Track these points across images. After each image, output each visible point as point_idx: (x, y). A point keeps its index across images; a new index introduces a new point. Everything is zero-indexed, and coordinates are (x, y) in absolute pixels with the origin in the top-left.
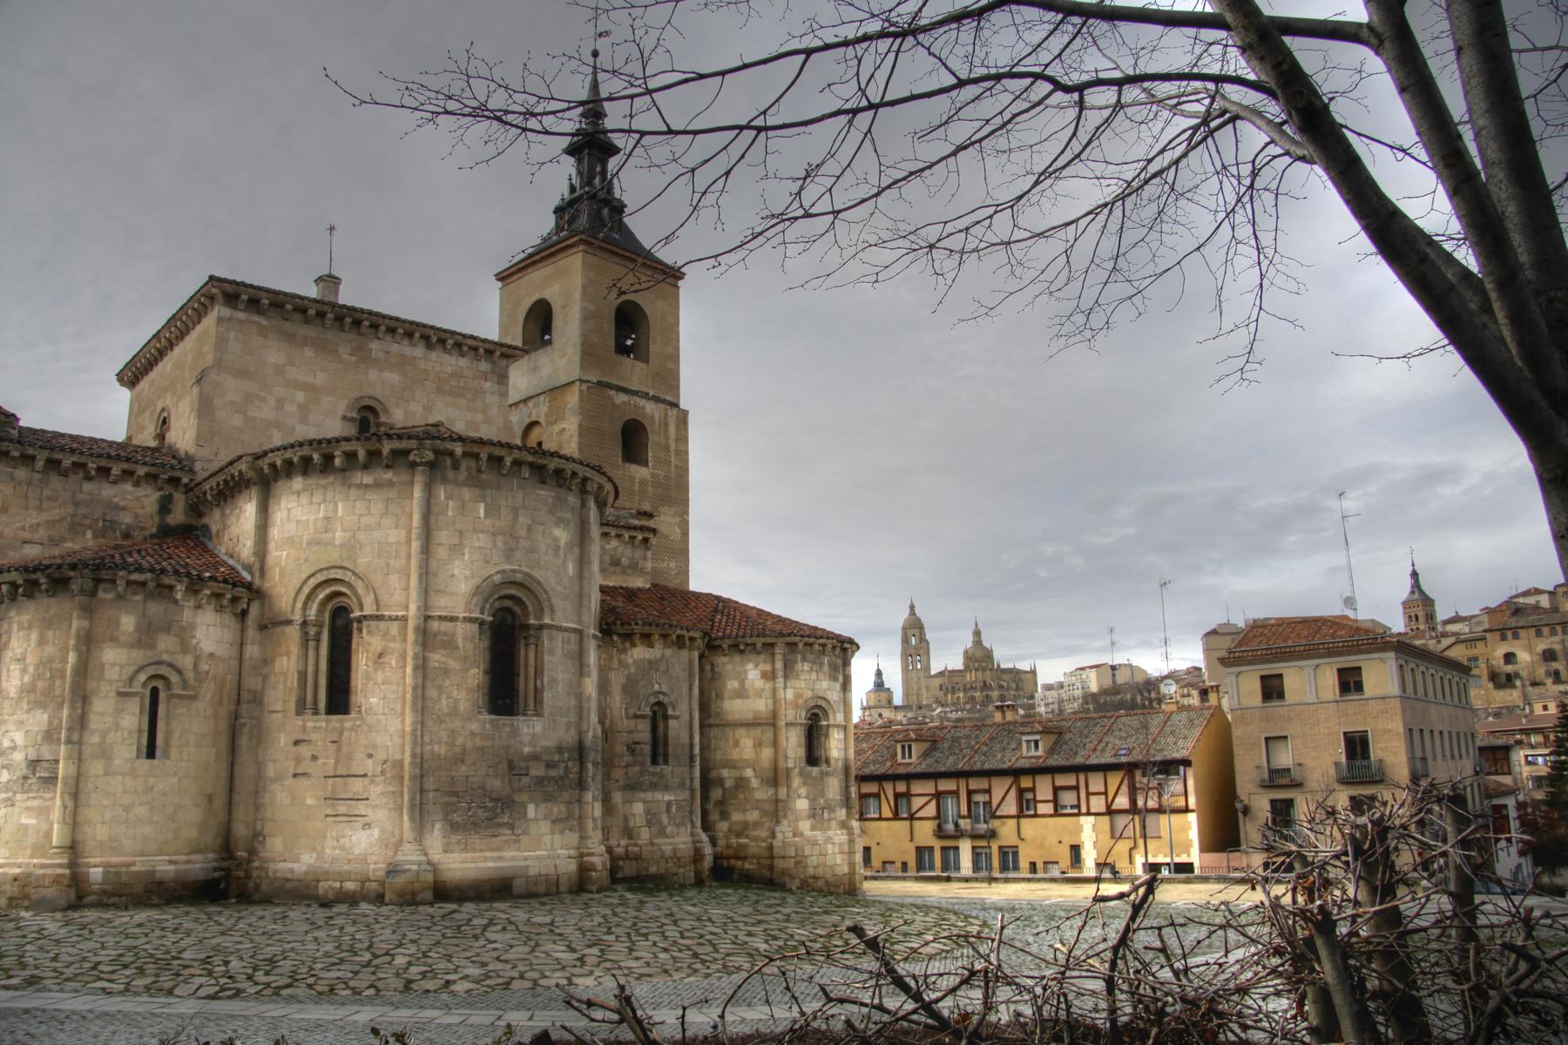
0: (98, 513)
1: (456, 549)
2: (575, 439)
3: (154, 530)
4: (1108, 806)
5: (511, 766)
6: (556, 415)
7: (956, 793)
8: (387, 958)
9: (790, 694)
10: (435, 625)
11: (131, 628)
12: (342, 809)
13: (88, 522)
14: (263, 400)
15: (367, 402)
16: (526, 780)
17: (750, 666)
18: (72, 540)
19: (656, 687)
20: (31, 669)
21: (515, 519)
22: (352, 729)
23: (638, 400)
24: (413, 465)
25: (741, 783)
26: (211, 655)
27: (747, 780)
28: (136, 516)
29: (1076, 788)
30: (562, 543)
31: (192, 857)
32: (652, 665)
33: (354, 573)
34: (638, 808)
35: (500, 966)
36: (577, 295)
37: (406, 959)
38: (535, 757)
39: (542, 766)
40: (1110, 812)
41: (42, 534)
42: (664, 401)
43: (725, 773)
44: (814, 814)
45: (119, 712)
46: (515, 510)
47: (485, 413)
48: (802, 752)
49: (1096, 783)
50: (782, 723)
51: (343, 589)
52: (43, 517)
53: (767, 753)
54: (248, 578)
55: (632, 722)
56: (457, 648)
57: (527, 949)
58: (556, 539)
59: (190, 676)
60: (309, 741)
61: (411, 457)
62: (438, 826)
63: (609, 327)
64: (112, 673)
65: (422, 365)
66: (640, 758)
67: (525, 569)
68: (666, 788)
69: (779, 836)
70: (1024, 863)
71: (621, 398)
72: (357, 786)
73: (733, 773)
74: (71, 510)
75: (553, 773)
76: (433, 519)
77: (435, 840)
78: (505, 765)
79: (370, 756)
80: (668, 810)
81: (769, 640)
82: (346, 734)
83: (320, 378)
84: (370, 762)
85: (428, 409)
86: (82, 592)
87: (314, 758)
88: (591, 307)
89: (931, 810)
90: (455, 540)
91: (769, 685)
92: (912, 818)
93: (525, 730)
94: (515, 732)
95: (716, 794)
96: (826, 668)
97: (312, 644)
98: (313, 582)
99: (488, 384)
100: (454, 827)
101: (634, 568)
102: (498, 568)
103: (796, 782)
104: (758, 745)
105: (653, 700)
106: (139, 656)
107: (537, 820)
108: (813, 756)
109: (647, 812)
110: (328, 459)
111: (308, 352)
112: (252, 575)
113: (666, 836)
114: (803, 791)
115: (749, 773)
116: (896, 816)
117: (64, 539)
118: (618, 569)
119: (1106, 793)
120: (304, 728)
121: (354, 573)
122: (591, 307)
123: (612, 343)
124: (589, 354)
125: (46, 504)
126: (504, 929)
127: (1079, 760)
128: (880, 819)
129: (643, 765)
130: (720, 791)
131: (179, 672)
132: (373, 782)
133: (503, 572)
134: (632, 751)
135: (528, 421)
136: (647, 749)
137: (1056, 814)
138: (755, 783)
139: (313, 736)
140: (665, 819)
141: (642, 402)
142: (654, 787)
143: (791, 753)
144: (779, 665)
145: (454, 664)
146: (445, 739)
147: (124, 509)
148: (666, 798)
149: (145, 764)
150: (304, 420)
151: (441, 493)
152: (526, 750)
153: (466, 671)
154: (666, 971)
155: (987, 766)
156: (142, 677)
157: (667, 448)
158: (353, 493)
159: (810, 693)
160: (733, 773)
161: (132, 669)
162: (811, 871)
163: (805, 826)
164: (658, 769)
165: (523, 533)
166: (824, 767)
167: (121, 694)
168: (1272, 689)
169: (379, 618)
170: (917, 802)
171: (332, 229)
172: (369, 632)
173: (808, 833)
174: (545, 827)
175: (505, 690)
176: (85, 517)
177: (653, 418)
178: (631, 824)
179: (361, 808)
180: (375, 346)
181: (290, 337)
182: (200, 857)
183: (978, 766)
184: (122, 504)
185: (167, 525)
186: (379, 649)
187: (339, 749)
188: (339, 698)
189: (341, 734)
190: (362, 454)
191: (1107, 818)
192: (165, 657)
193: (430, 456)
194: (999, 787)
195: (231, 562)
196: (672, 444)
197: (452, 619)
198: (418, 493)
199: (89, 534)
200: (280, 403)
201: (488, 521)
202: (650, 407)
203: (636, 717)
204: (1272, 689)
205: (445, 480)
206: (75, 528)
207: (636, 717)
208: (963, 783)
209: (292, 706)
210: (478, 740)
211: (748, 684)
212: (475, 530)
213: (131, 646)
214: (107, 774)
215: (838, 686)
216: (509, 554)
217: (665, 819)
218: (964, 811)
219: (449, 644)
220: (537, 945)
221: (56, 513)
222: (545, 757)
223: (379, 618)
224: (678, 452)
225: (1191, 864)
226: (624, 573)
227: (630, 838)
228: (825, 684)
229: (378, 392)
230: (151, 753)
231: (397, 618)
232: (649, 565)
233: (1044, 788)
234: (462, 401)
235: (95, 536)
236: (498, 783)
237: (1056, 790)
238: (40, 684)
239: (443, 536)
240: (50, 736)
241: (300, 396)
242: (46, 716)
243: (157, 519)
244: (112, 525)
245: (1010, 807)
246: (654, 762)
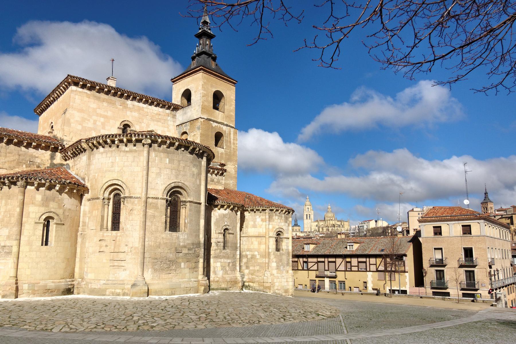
0: (28, 159)
1: (159, 174)
2: (199, 138)
3: (49, 165)
4: (377, 269)
5: (176, 248)
6: (192, 129)
7: (324, 262)
8: (131, 317)
9: (271, 227)
10: (150, 200)
11: (40, 200)
13: (24, 161)
14: (89, 120)
15: (126, 123)
16: (181, 254)
17: (258, 217)
18: (18, 168)
19: (226, 223)
21: (179, 164)
22: (120, 236)
24: (144, 145)
25: (253, 257)
26: (70, 209)
27: (256, 256)
28: (42, 160)
29: (365, 262)
30: (195, 173)
31: (61, 280)
32: (224, 216)
34: (219, 264)
35: (171, 320)
36: (200, 88)
37: (138, 318)
38: (185, 247)
39: (187, 250)
40: (377, 271)
41: (6, 165)
42: (230, 126)
43: (248, 253)
44: (278, 268)
45: (35, 229)
46: (179, 161)
47: (168, 128)
48: (274, 247)
49: (373, 260)
50: (267, 237)
51: (118, 187)
52: (7, 159)
53: (263, 247)
54: (84, 183)
55: (217, 235)
56: (158, 208)
57: (181, 314)
58: (193, 172)
59: (62, 217)
61: (143, 142)
62: (150, 270)
63: (211, 99)
64: (32, 215)
65: (146, 110)
66: (219, 247)
67: (182, 182)
69: (266, 275)
70: (347, 287)
71: (214, 124)
72: (122, 256)
73: (251, 253)
74: (17, 157)
75: (190, 252)
76: (150, 163)
77: (148, 275)
78: (174, 249)
79: (127, 245)
80: (229, 265)
81: (264, 208)
82: (118, 238)
83: (109, 114)
84: (126, 247)
85: (148, 125)
86: (21, 186)
87: (106, 246)
88: (205, 92)
89: (315, 267)
90: (158, 171)
91: (264, 223)
92: (308, 270)
93: (181, 237)
94: (178, 238)
95: (244, 260)
96: (283, 218)
97: (106, 206)
98: (107, 185)
99: (169, 118)
100: (155, 270)
101: (218, 182)
102: (173, 181)
103: (272, 257)
104: (260, 243)
105: (224, 228)
106: (43, 210)
107: (184, 268)
108: (278, 250)
109: (221, 266)
110: (113, 142)
111: (105, 104)
112: (84, 181)
113: (228, 274)
114: (274, 260)
115: (256, 253)
116: (303, 270)
117: (14, 168)
118: (213, 183)
119: (376, 264)
120: (103, 236)
122: (205, 92)
123: (212, 105)
124: (204, 109)
125: (8, 155)
126: (172, 306)
127: (366, 253)
128: (298, 270)
129: (220, 250)
130: (246, 259)
131: (58, 215)
132: (127, 254)
133: (175, 182)
134: (217, 245)
135: (183, 131)
136: (222, 244)
137: (358, 271)
138: (258, 257)
139: (106, 238)
140: (227, 268)
141: (222, 126)
142: (224, 257)
143: (270, 247)
144: (267, 217)
145: (156, 214)
146: (153, 240)
147: (37, 157)
148: (228, 261)
149: (44, 247)
150: (104, 128)
151: (153, 154)
152: (181, 244)
153: (162, 216)
154: (229, 323)
155: (335, 253)
156: (44, 217)
157: (230, 142)
158: (122, 154)
159: (277, 227)
160: (251, 253)
161: (42, 214)
162: (276, 288)
163: (275, 272)
165: (182, 169)
166: (281, 251)
167: (36, 223)
168: (438, 231)
169: (131, 197)
170: (310, 265)
172: (127, 202)
173: (276, 275)
174: (187, 270)
175: (173, 224)
176: (23, 160)
177: (225, 132)
178: (216, 270)
179: (123, 263)
180: (129, 102)
181: (99, 99)
182: (64, 280)
183: (332, 253)
184: (37, 155)
185: (54, 164)
186: (131, 208)
187: (116, 243)
188: (116, 225)
189: (116, 238)
190: (125, 140)
191: (377, 273)
192: (52, 210)
193: (149, 141)
194: (339, 260)
195: (77, 177)
196: (232, 141)
197: (157, 198)
198: (145, 153)
199: (24, 166)
200: (95, 122)
201: (170, 165)
202: (224, 128)
203: (219, 233)
204: (438, 231)
205: (155, 150)
206: (19, 163)
207: (219, 233)
208: (326, 259)
209: (99, 228)
210: (165, 241)
211: (256, 223)
212: (165, 168)
213: (40, 206)
214: (30, 251)
215: (287, 225)
216: (177, 176)
217: (227, 268)
218: (326, 268)
219: (156, 207)
220: (184, 313)
221: (12, 158)
222: (188, 247)
223: (131, 197)
224: (234, 144)
225: (406, 291)
226: (215, 184)
227: (215, 274)
228: (283, 224)
229: (130, 119)
230: (46, 244)
231: (137, 198)
232: (223, 182)
233: (354, 261)
234: (160, 124)
235: (26, 167)
236: (171, 255)
237: (359, 262)
238: (5, 219)
239: (153, 170)
240: (8, 237)
241: (102, 120)
242: (8, 230)
243: (50, 161)
244: (32, 162)
245: (342, 268)
246: (224, 248)
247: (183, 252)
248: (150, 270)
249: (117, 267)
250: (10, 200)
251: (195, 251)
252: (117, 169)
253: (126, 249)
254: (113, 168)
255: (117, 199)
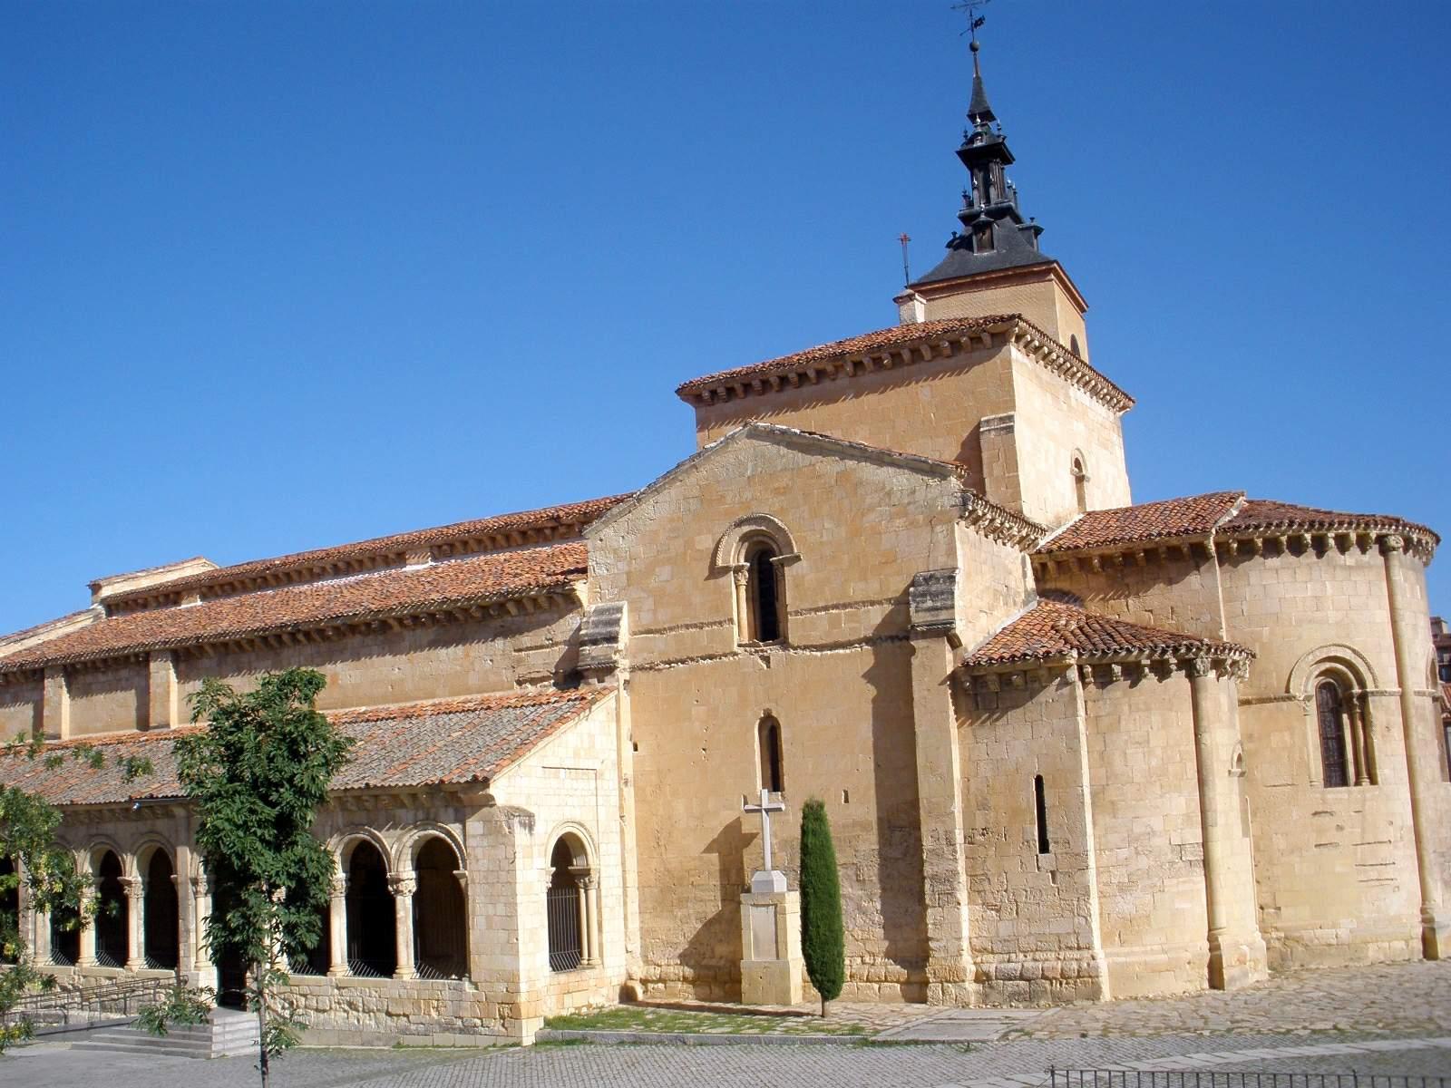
12: (1373, 874)
20: (1159, 752)
33: (1354, 651)
60: (1331, 814)
82: (1368, 803)
84: (1391, 828)
120: (1324, 801)
121: (1354, 651)
132: (1395, 847)
158: (1340, 574)
171: (905, 239)
172: (1374, 708)
179: (1389, 872)
189: (1364, 805)
223: (1382, 693)
242: (1182, 800)
248: (1439, 884)
249: (1377, 883)
250: (1174, 714)
252: (1332, 616)
253: (1391, 834)
254: (1318, 614)
255: (1342, 698)
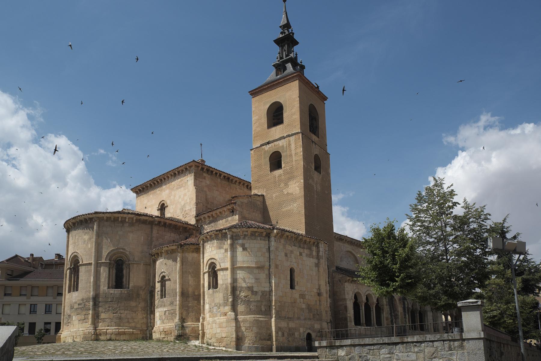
23: (275, 143)
38: (76, 303)
68: (164, 306)
71: (267, 148)
75: (80, 306)
96: (215, 245)
152: (74, 301)
164: (162, 300)
177: (283, 146)
196: (293, 152)
202: (280, 143)
215: (223, 251)
228: (215, 252)
247: (75, 307)
251: (85, 305)
